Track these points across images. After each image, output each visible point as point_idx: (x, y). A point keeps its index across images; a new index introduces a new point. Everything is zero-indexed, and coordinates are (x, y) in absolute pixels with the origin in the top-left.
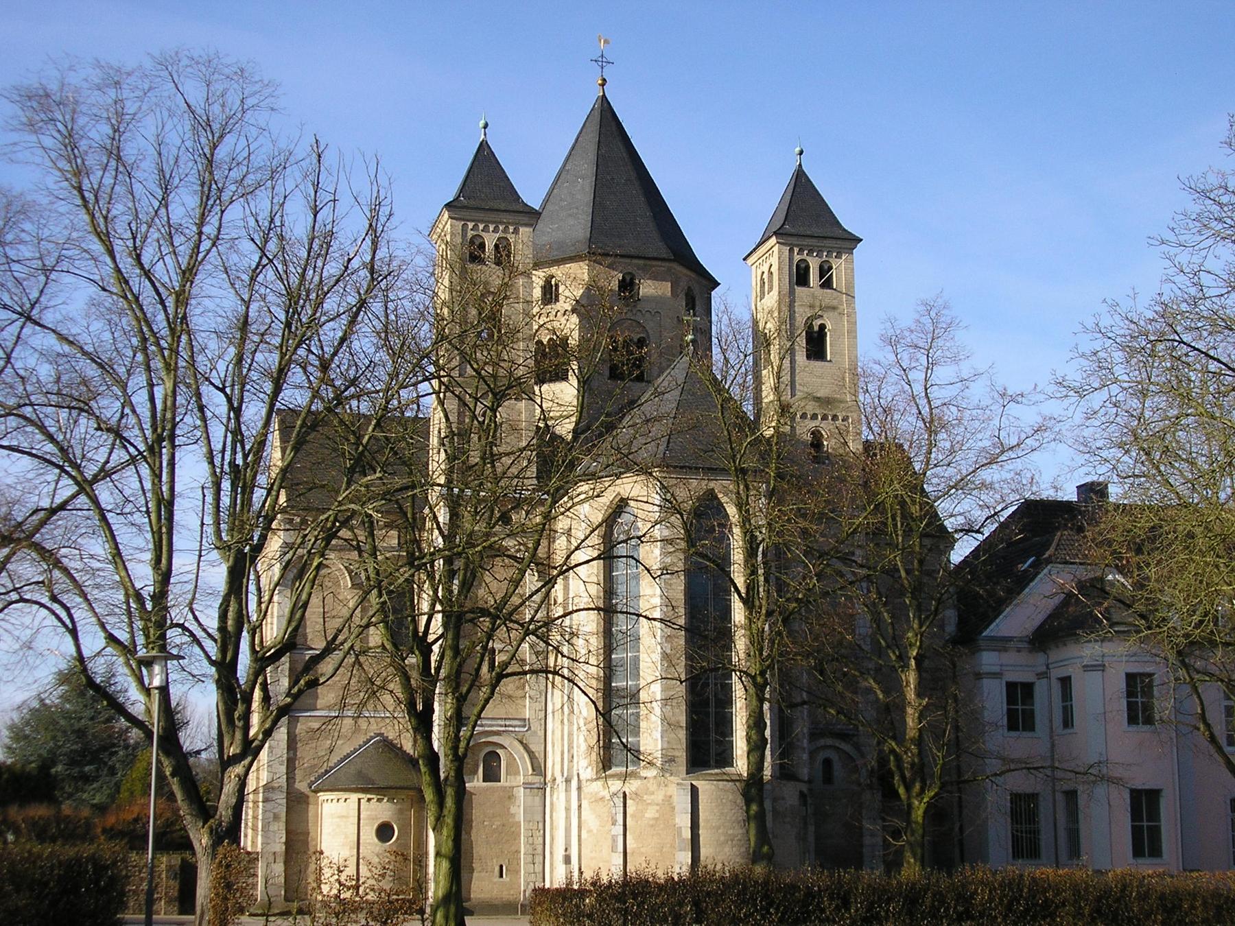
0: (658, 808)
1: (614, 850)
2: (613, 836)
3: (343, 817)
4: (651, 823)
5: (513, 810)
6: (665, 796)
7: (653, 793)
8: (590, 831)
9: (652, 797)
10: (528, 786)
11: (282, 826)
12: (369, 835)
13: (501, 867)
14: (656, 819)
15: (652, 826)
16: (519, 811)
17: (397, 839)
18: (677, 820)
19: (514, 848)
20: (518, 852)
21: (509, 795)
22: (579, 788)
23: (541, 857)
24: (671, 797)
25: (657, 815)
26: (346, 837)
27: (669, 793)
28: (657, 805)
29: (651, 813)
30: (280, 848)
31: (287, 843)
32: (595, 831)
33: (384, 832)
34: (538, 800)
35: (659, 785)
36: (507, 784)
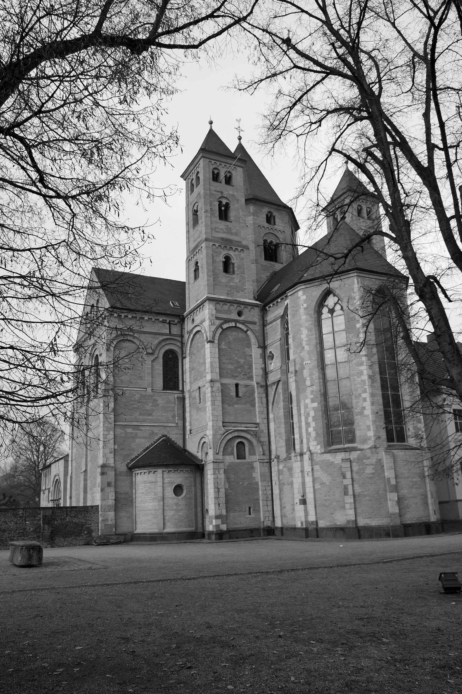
0: (373, 467)
1: (346, 493)
2: (344, 486)
3: (153, 482)
4: (370, 476)
5: (254, 475)
6: (377, 459)
7: (369, 458)
8: (322, 484)
9: (369, 460)
10: (261, 462)
11: (112, 489)
12: (170, 492)
13: (250, 508)
14: (373, 474)
15: (370, 478)
16: (257, 475)
17: (186, 494)
18: (386, 474)
19: (255, 497)
20: (258, 499)
21: (251, 467)
22: (311, 459)
23: (271, 502)
24: (380, 460)
25: (373, 471)
26: (156, 494)
27: (379, 458)
28: (373, 465)
29: (369, 470)
30: (111, 502)
31: (115, 500)
32: (328, 483)
33: (178, 490)
34: (267, 469)
35: (372, 453)
36: (250, 461)
